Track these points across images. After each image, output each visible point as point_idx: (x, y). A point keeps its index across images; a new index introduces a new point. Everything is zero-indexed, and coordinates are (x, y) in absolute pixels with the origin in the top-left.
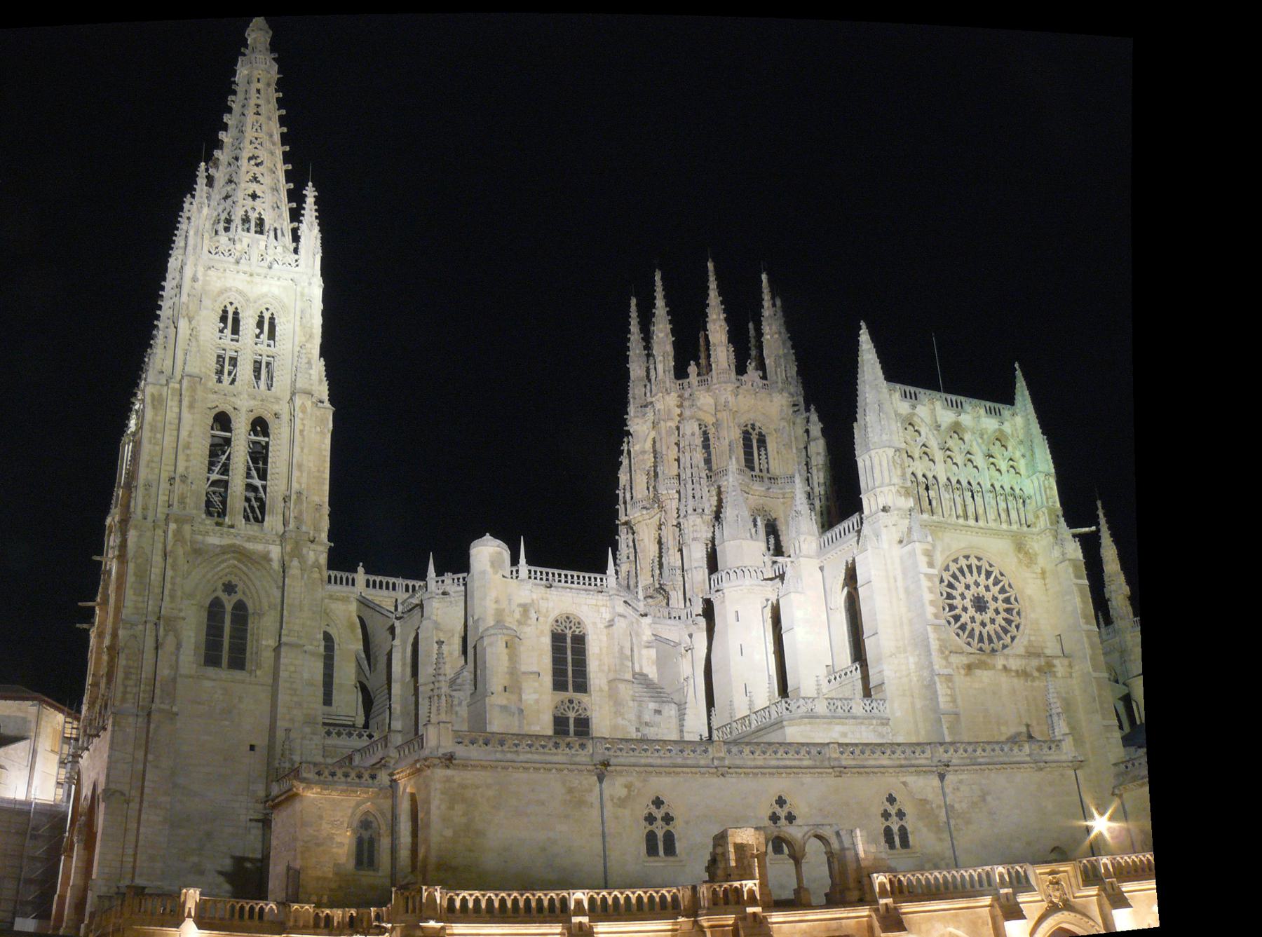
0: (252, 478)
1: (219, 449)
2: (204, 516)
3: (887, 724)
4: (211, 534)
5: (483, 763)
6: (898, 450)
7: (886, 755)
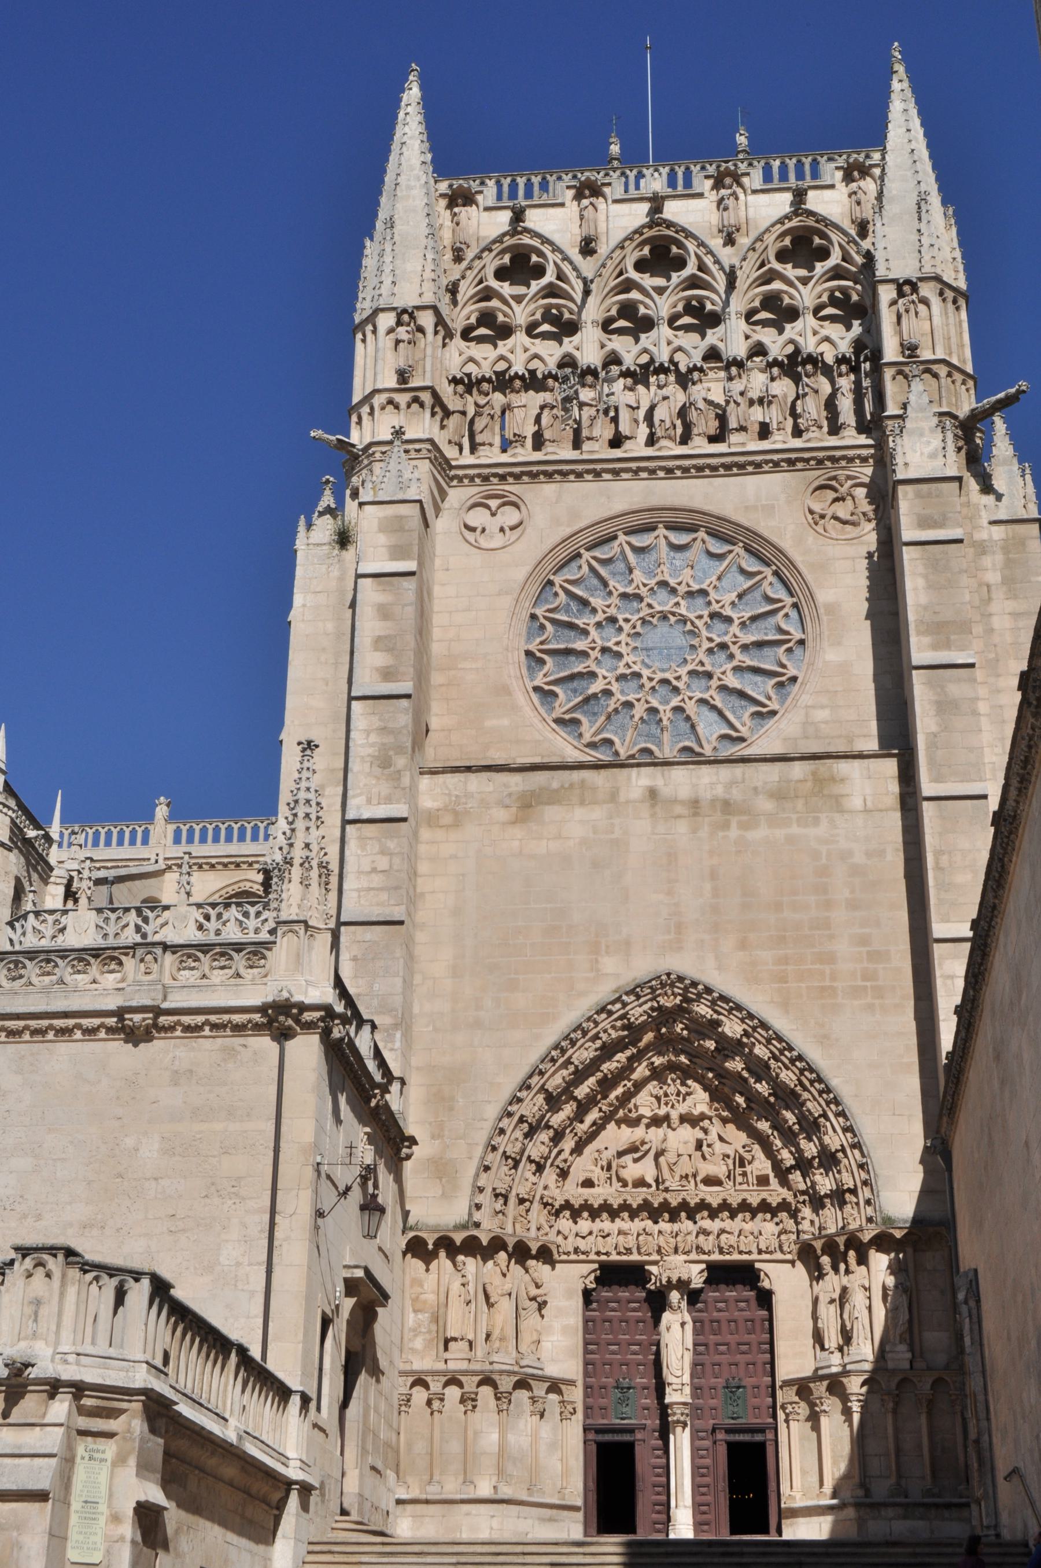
6: (405, 315)
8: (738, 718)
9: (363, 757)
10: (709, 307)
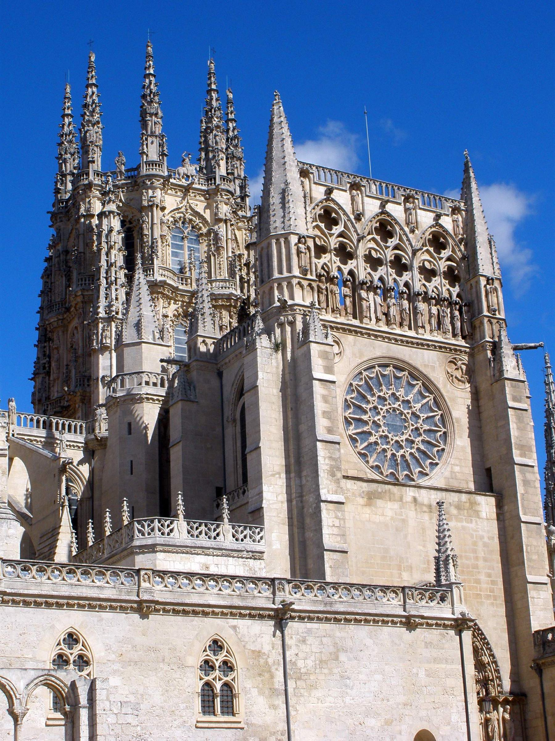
6: (301, 239)
8: (424, 464)
9: (324, 470)
10: (404, 261)
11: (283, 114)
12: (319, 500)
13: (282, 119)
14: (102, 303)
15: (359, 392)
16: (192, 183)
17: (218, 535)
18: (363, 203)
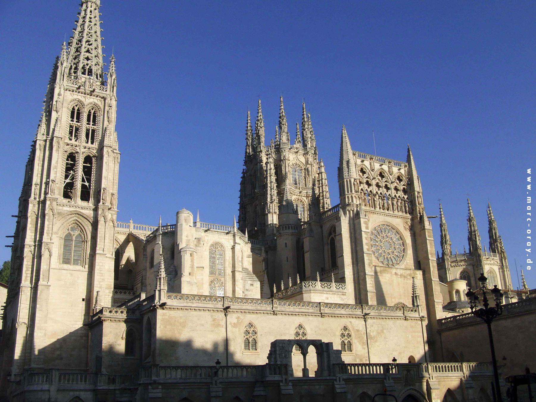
0: (85, 182)
1: (70, 168)
2: (63, 198)
3: (345, 295)
4: (65, 206)
5: (178, 307)
7: (344, 309)
10: (388, 186)
11: (346, 133)
12: (365, 274)
13: (346, 135)
14: (269, 196)
15: (375, 235)
16: (299, 151)
17: (331, 287)
18: (374, 165)
